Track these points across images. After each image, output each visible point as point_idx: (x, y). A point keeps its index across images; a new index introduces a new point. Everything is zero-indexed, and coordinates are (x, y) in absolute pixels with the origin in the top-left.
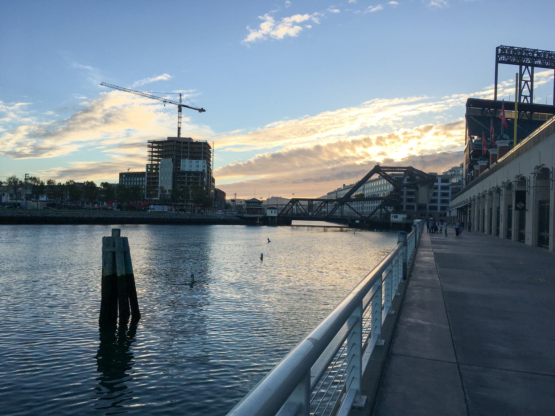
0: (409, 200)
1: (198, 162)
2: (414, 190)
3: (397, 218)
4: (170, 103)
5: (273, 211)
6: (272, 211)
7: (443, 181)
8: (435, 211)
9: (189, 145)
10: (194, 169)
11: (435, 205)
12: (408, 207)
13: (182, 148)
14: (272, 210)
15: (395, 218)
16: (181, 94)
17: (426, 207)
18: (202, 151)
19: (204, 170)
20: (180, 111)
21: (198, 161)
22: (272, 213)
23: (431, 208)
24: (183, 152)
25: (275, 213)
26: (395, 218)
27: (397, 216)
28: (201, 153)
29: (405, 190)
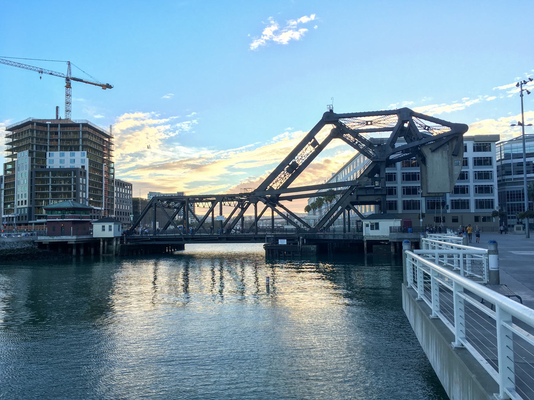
0: (408, 191)
1: (73, 155)
2: (416, 170)
3: (377, 228)
4: (51, 74)
5: (107, 225)
6: (103, 227)
7: (477, 148)
8: (466, 211)
9: (59, 129)
10: (67, 165)
11: (463, 197)
12: (407, 205)
13: (48, 133)
14: (103, 224)
15: (372, 228)
16: (69, 62)
17: (444, 203)
18: (81, 136)
19: (83, 167)
20: (68, 86)
21: (74, 153)
22: (104, 230)
23: (456, 205)
24: (51, 140)
25: (110, 230)
26: (372, 228)
27: (377, 224)
28: (78, 140)
29: (399, 169)
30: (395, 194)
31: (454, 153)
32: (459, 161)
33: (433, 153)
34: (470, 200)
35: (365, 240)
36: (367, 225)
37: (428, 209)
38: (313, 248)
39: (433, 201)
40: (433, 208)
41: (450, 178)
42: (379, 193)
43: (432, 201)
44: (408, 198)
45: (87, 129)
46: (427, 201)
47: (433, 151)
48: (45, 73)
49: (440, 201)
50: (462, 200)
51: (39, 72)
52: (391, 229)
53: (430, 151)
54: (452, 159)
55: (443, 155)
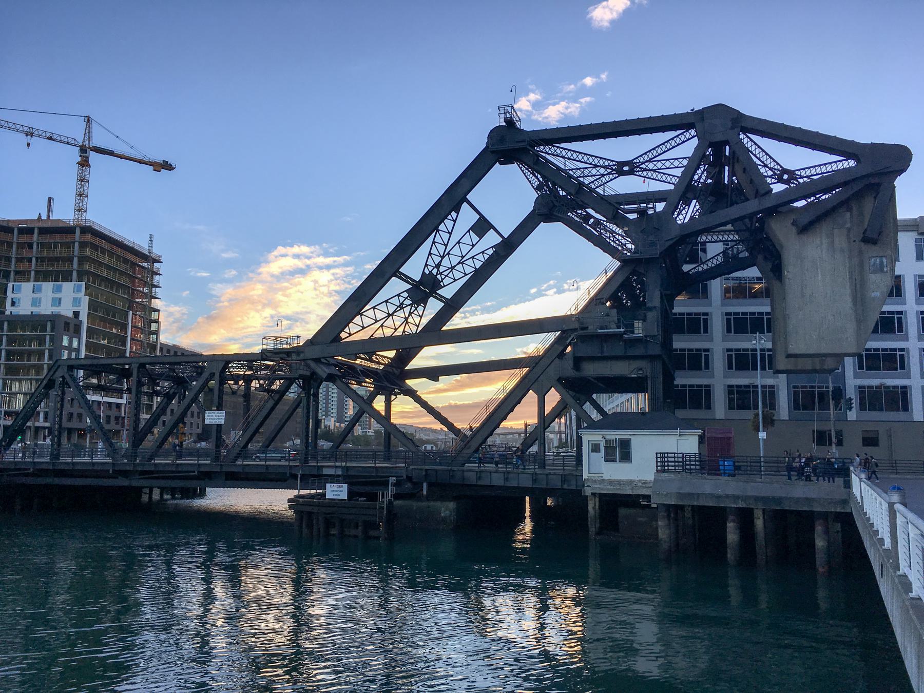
1: (58, 290)
3: (626, 457)
4: (50, 138)
8: (900, 415)
9: (35, 237)
10: (46, 309)
13: (14, 246)
16: (89, 117)
17: (839, 393)
18: (76, 253)
19: (76, 314)
20: (84, 163)
21: (61, 286)
24: (19, 260)
26: (610, 458)
28: (71, 260)
30: (707, 367)
31: (869, 234)
32: (885, 261)
33: (804, 237)
34: (910, 387)
35: (588, 492)
36: (595, 448)
38: (447, 509)
40: (808, 406)
41: (855, 311)
42: (639, 351)
43: (806, 387)
44: (742, 380)
45: (89, 237)
46: (794, 387)
47: (805, 229)
48: (39, 136)
49: (827, 387)
50: (888, 387)
51: (27, 135)
52: (663, 462)
53: (794, 230)
54: (861, 252)
55: (833, 242)
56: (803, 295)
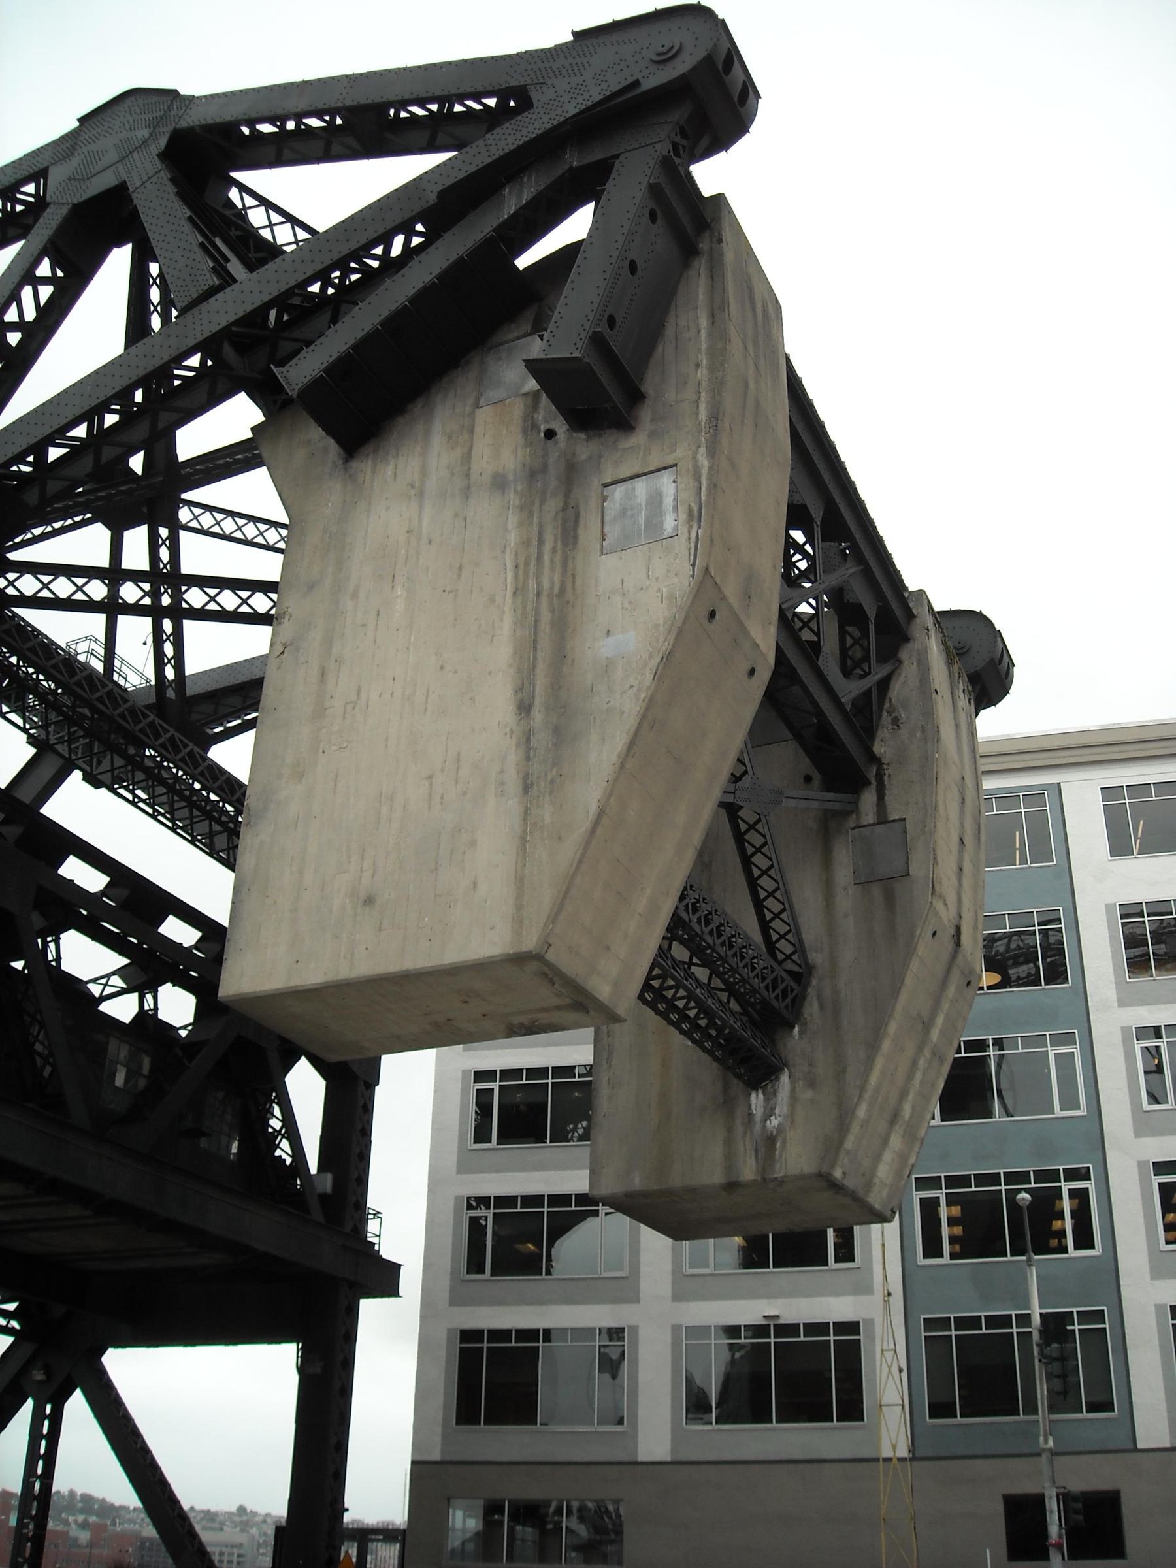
33: (363, 466)
37: (940, 1409)
39: (993, 1321)
43: (974, 1322)
56: (319, 712)
